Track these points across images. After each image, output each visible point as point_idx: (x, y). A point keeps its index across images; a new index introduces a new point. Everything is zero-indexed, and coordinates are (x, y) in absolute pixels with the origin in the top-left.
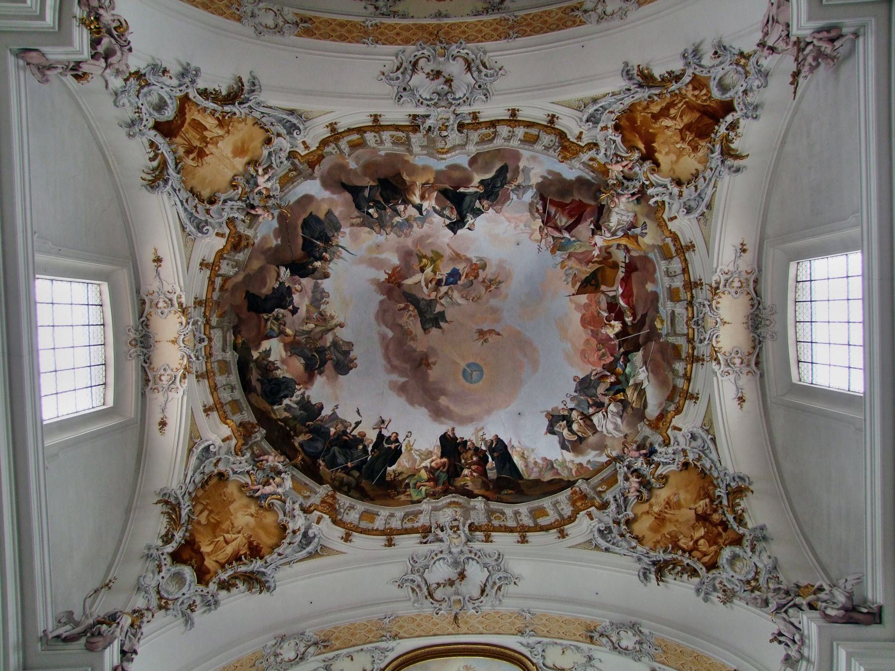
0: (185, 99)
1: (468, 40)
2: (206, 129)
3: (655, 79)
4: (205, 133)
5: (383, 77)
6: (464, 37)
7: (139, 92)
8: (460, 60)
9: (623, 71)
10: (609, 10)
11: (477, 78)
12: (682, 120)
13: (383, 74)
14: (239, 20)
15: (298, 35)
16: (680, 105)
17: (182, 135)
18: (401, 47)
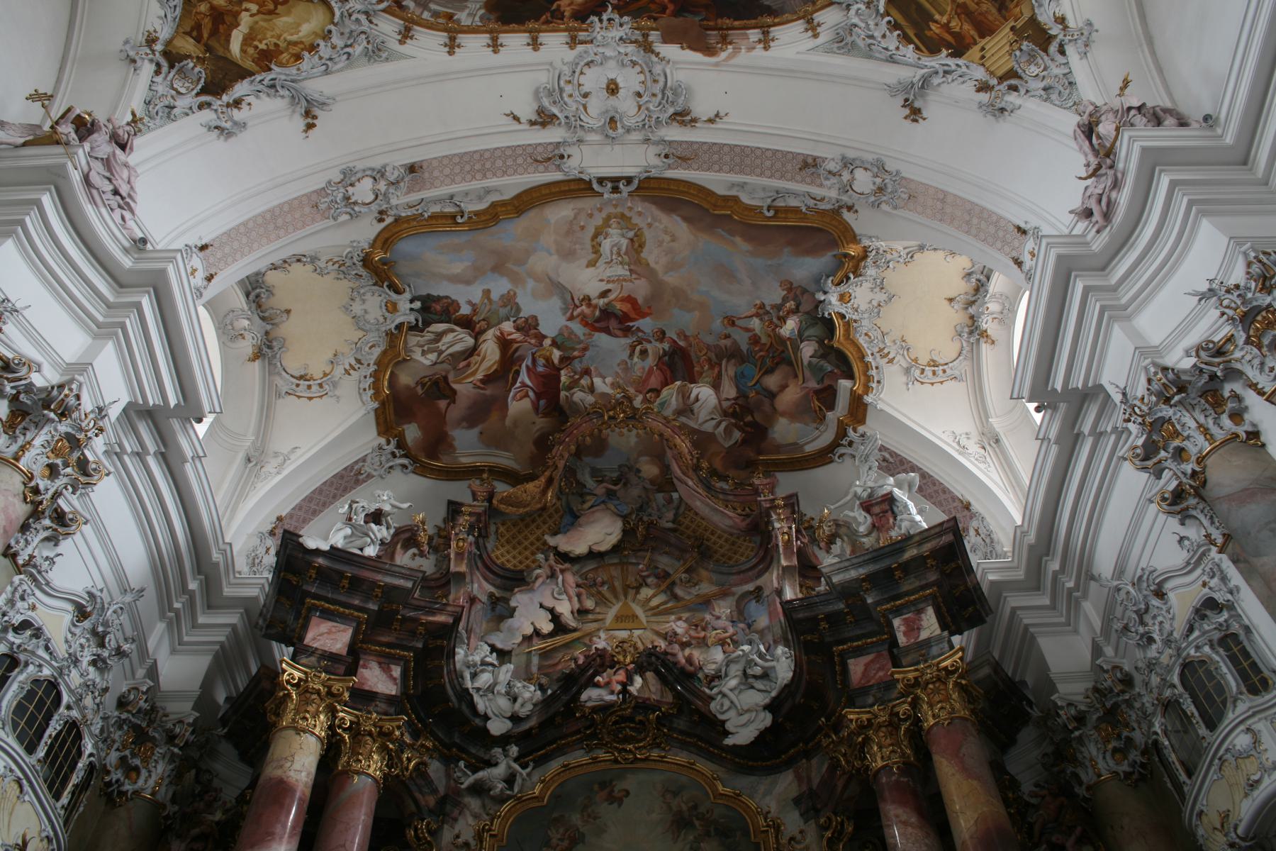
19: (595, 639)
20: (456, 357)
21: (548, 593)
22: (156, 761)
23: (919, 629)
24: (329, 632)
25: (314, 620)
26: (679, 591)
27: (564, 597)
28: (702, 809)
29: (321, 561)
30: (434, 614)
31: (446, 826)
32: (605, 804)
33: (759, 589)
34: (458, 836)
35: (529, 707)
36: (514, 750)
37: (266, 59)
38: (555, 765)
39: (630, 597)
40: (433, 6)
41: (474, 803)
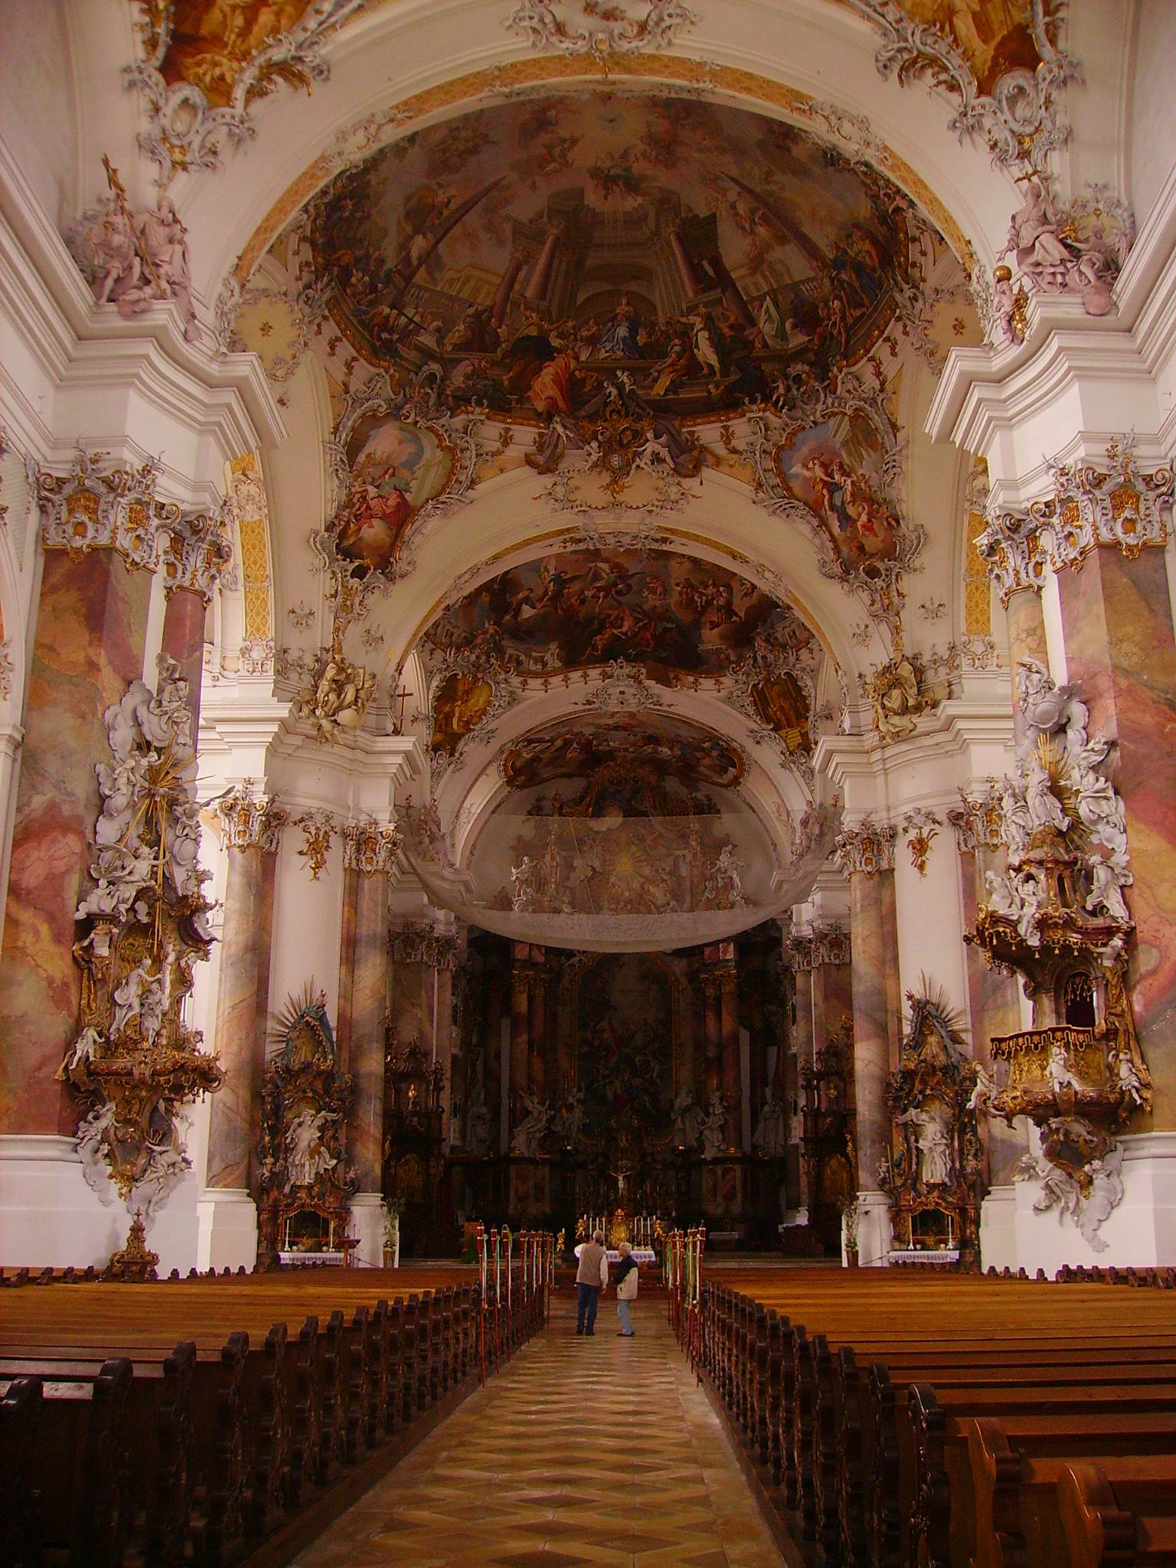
0: (983, 90)
1: (561, 58)
2: (975, 15)
3: (279, 74)
4: (977, 8)
5: (693, 19)
6: (567, 61)
7: (1037, 130)
8: (571, 33)
9: (329, 71)
10: (361, 134)
11: (546, 13)
12: (222, 11)
13: (692, 23)
14: (886, 148)
15: (811, 98)
16: (233, 37)
17: (1009, 23)
18: (663, 53)
20: (541, 751)
37: (467, 726)
40: (534, 654)
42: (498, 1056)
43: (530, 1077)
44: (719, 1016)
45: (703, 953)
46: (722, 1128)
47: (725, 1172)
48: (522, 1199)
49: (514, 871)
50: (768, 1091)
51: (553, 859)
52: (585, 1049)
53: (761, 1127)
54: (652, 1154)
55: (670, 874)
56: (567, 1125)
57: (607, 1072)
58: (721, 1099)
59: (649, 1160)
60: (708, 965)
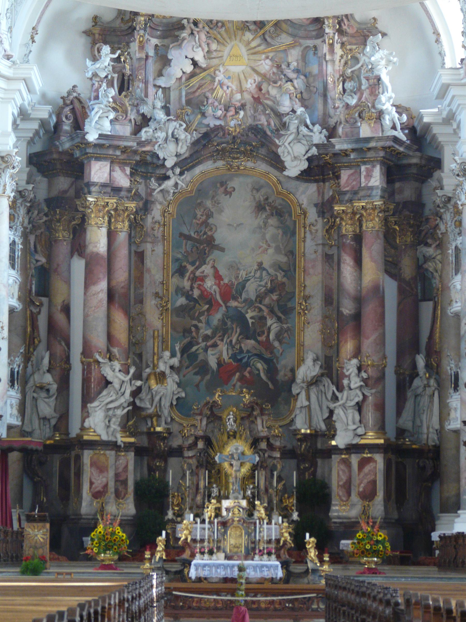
19: (217, 72)
21: (190, 48)
22: (19, 207)
23: (371, 176)
24: (100, 169)
25: (93, 162)
26: (267, 37)
27: (200, 49)
28: (270, 200)
29: (96, 142)
30: (144, 146)
31: (148, 215)
32: (223, 195)
33: (315, 47)
34: (153, 218)
35: (185, 148)
36: (178, 170)
38: (198, 170)
39: (238, 38)
41: (159, 197)
42: (66, 310)
43: (110, 338)
44: (358, 261)
45: (338, 177)
46: (359, 407)
47: (363, 463)
48: (97, 495)
49: (89, 63)
50: (421, 361)
51: (142, 47)
52: (182, 301)
53: (409, 405)
54: (268, 439)
55: (297, 71)
56: (157, 399)
57: (209, 332)
58: (360, 369)
59: (263, 445)
60: (345, 193)
